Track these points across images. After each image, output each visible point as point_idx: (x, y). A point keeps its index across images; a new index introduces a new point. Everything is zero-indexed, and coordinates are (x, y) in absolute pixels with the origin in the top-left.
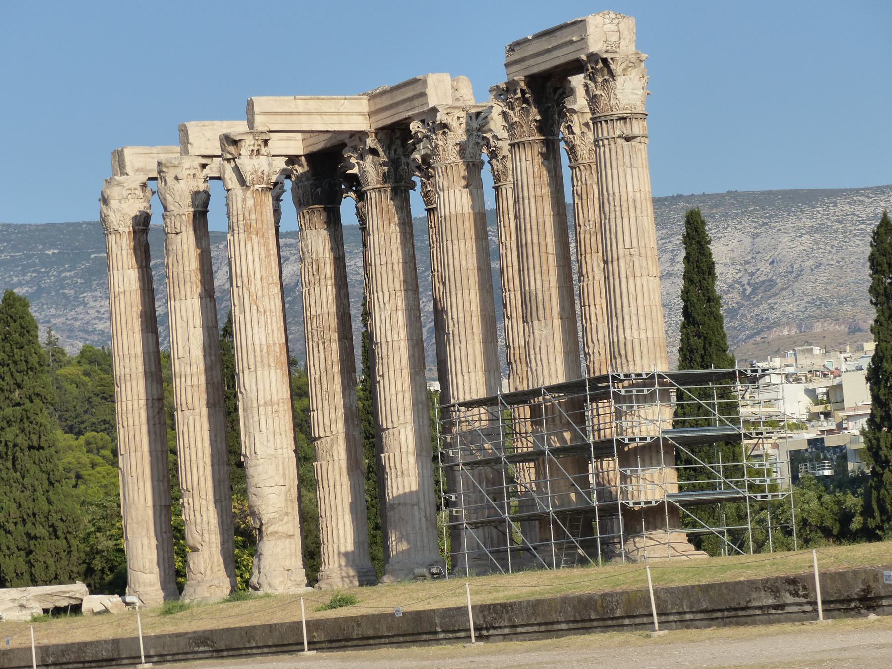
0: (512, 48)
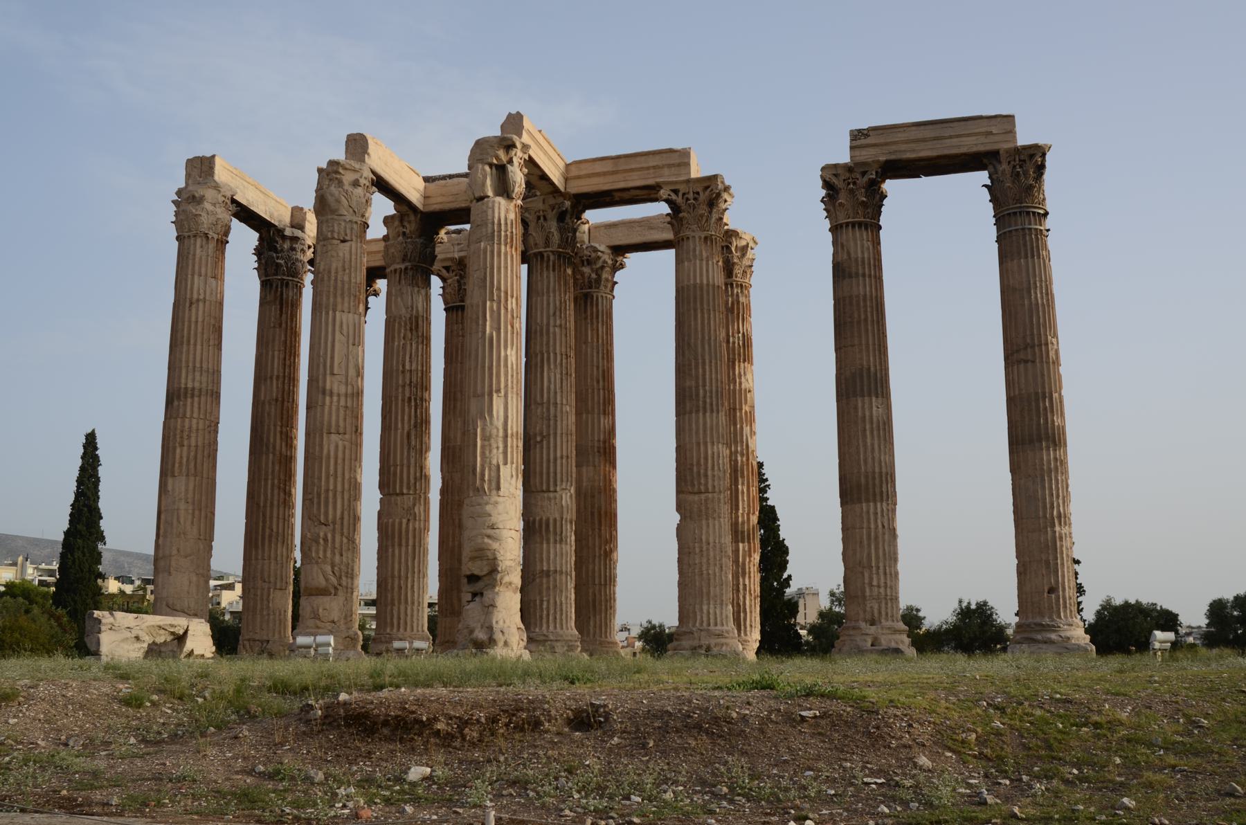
0: (858, 137)
